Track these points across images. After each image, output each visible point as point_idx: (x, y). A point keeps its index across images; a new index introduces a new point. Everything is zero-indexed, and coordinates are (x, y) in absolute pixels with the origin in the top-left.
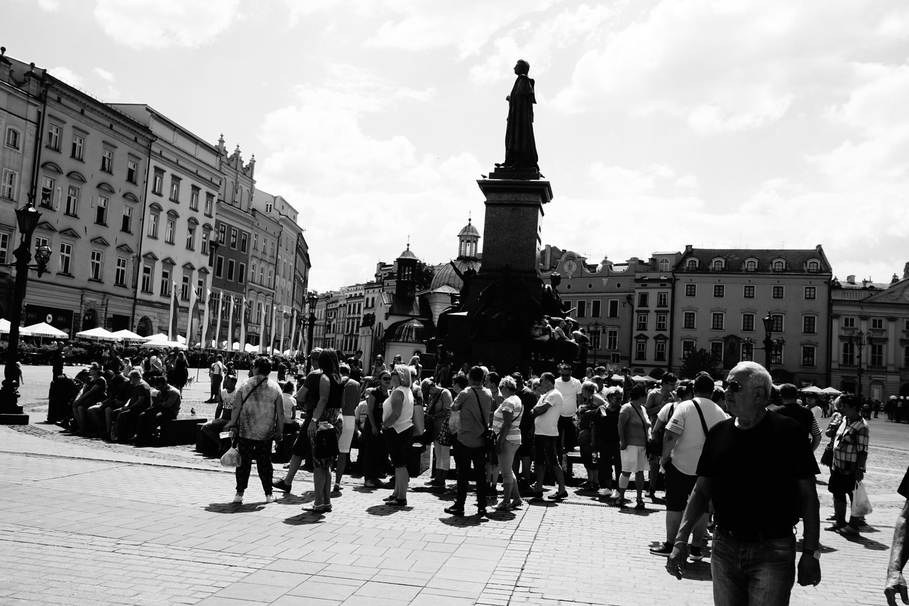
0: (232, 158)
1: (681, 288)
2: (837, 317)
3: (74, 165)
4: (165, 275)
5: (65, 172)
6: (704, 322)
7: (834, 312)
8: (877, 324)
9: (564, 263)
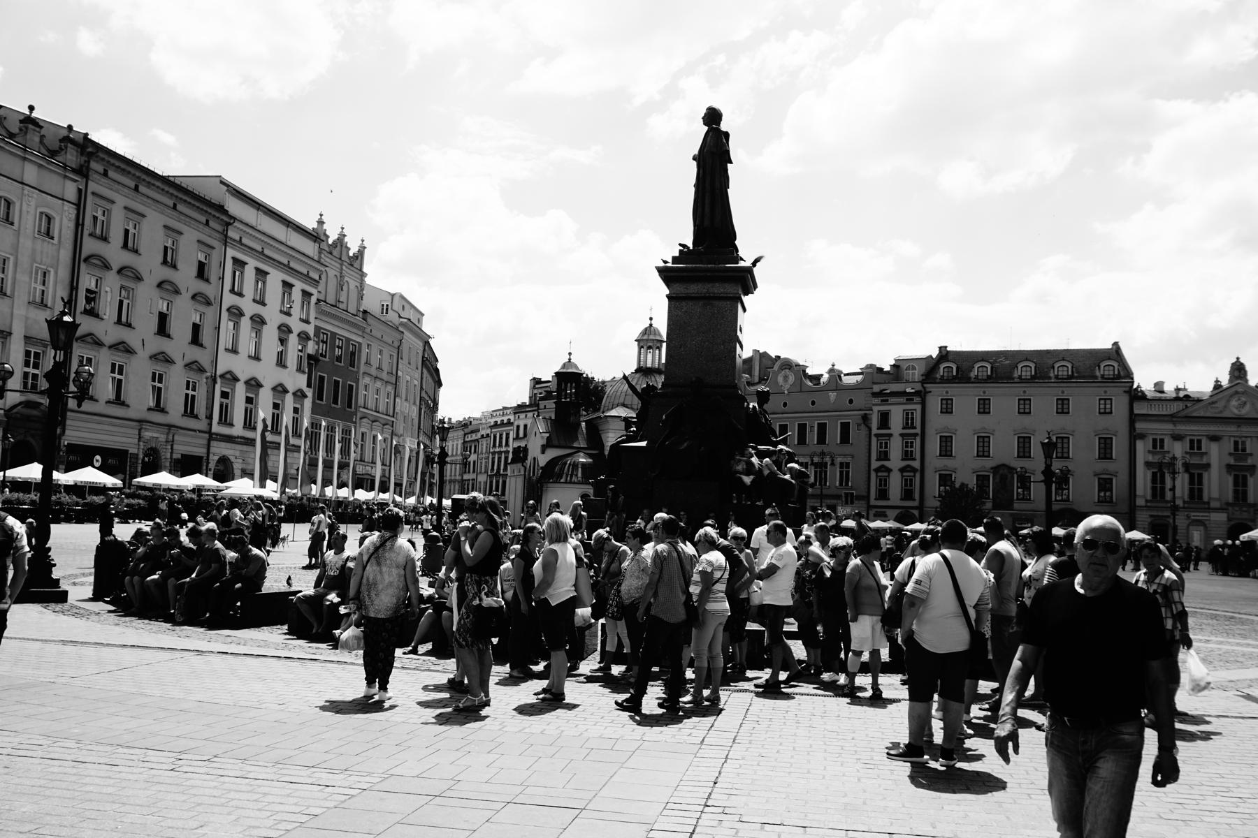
0: (335, 244)
1: (934, 403)
2: (1142, 436)
3: (126, 258)
4: (249, 400)
5: (115, 267)
6: (965, 447)
7: (1138, 431)
8: (1195, 445)
9: (777, 374)
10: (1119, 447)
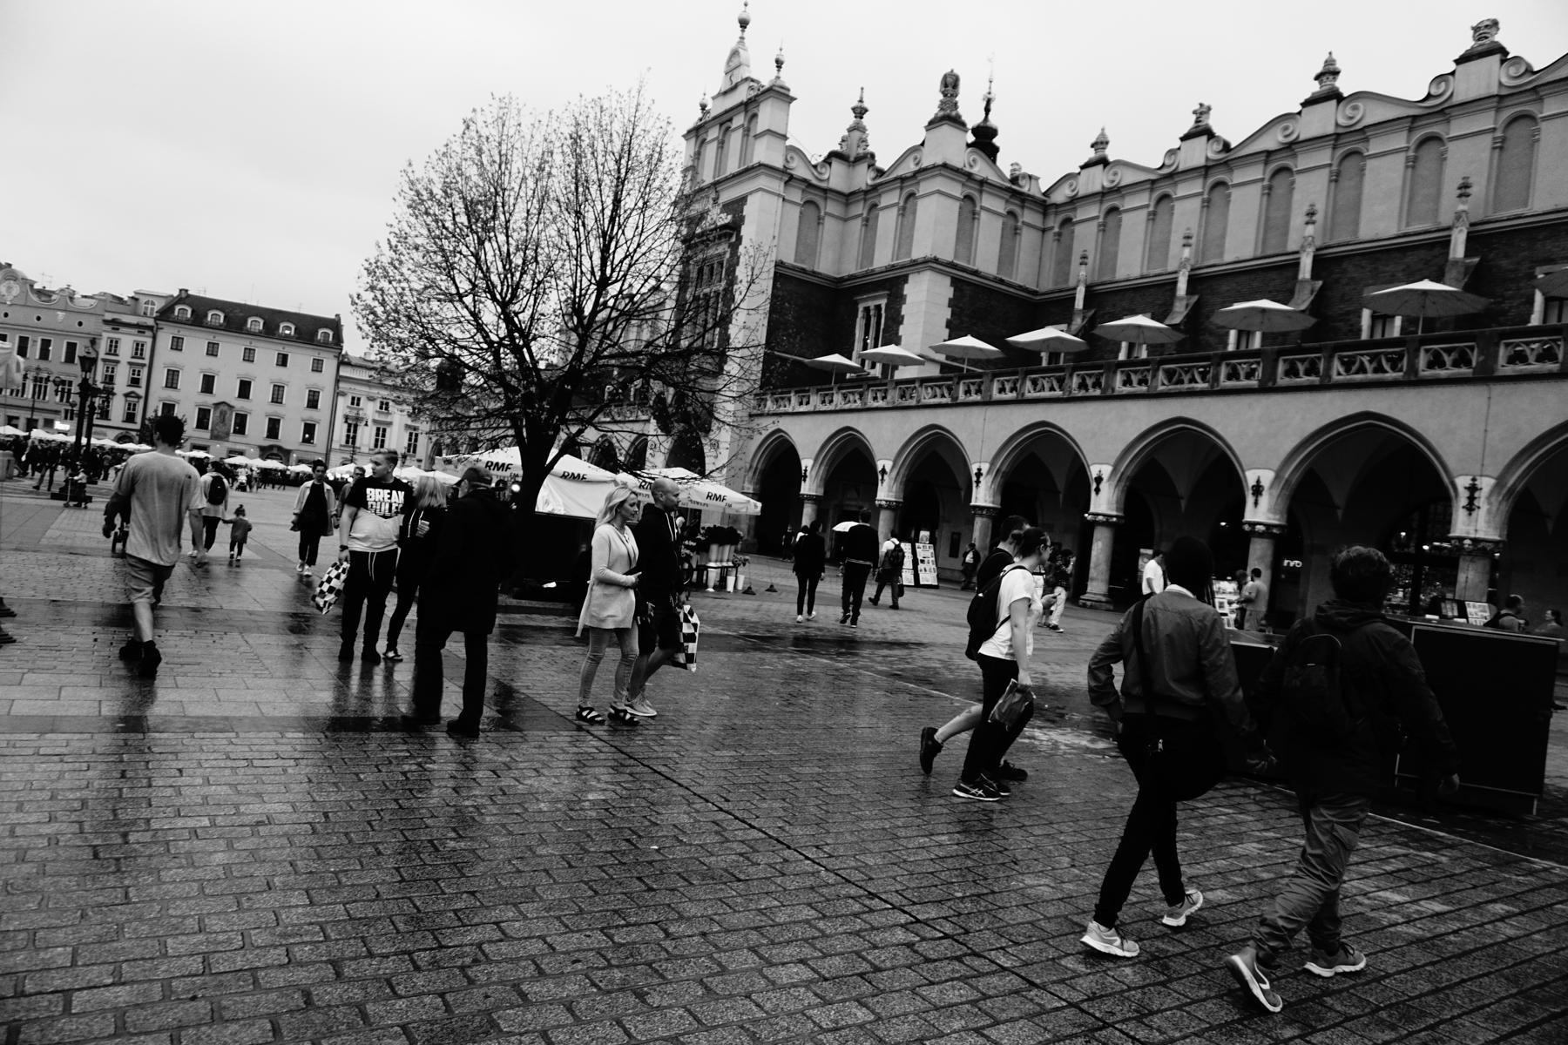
1: (165, 339)
2: (344, 394)
6: (190, 384)
8: (384, 406)
10: (324, 401)
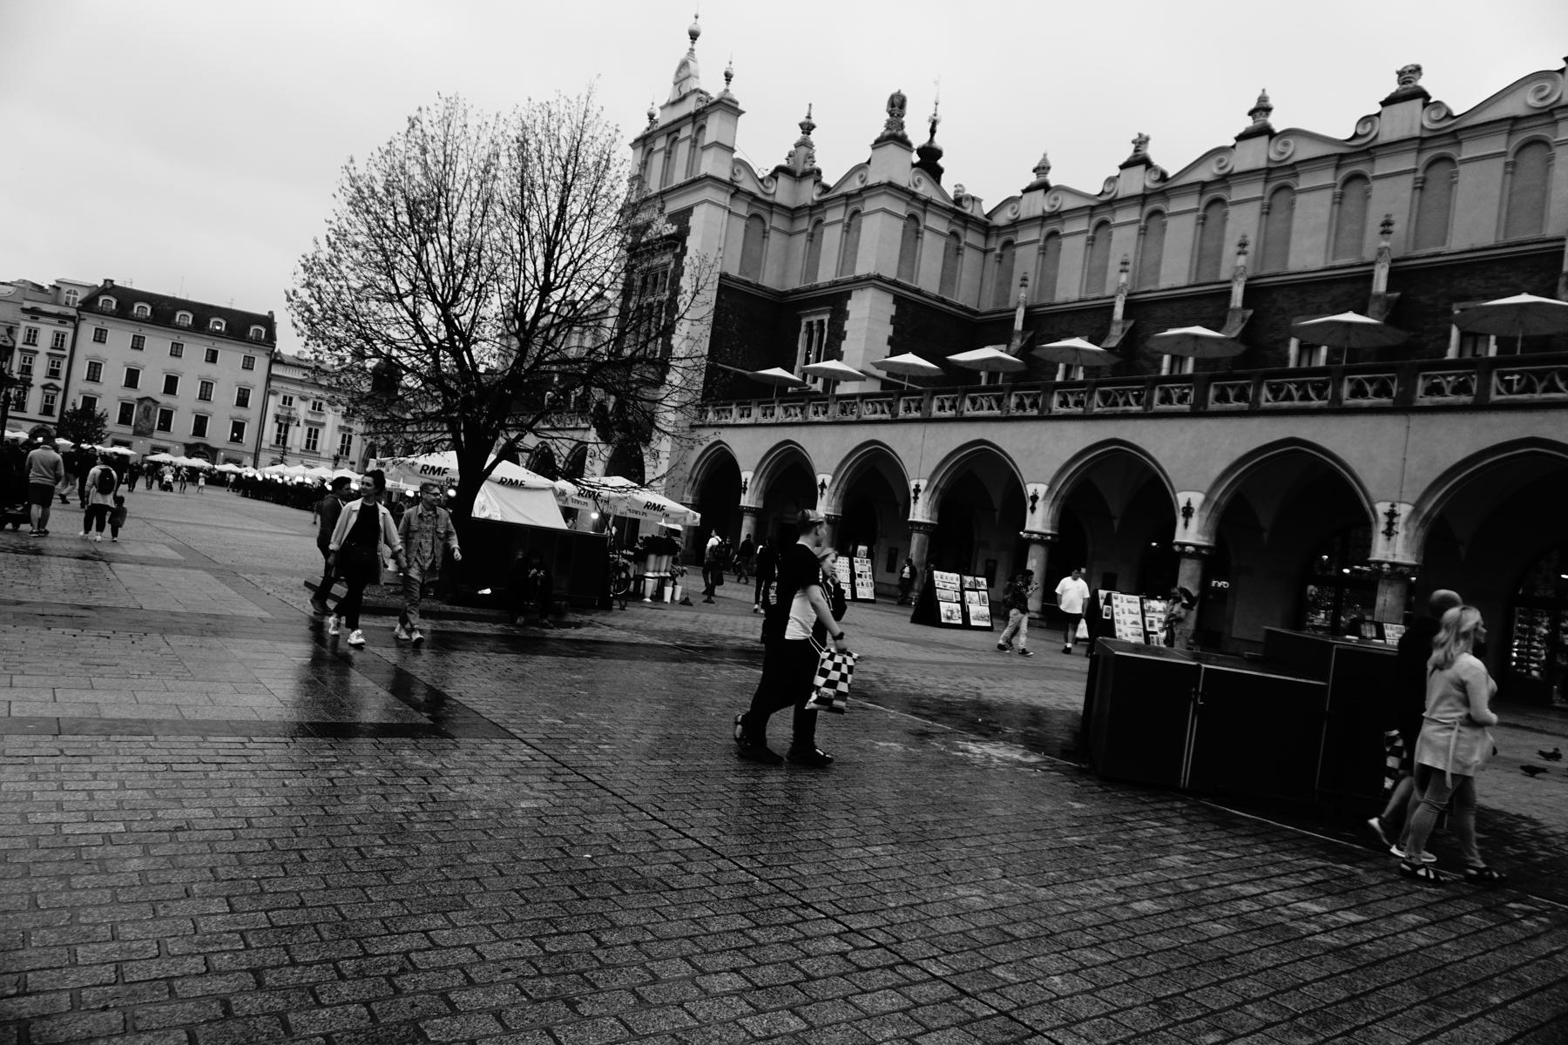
1: (87, 330)
2: (275, 393)
8: (317, 407)
10: (255, 399)
